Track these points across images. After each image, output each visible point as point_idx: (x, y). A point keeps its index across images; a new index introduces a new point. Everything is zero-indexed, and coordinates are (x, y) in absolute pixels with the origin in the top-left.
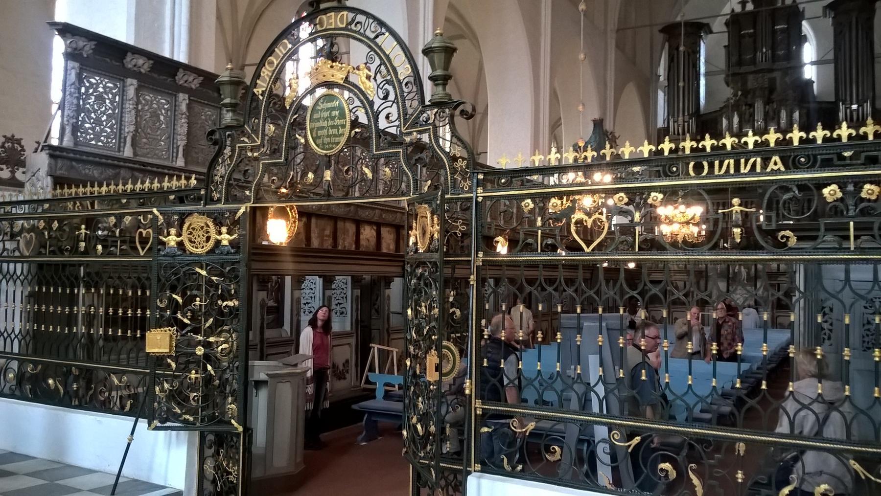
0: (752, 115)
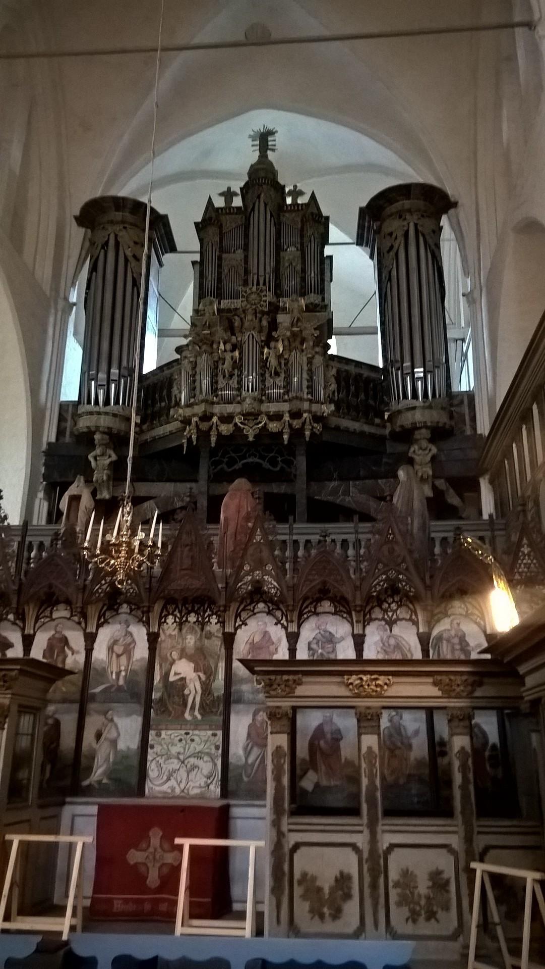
0: (238, 365)
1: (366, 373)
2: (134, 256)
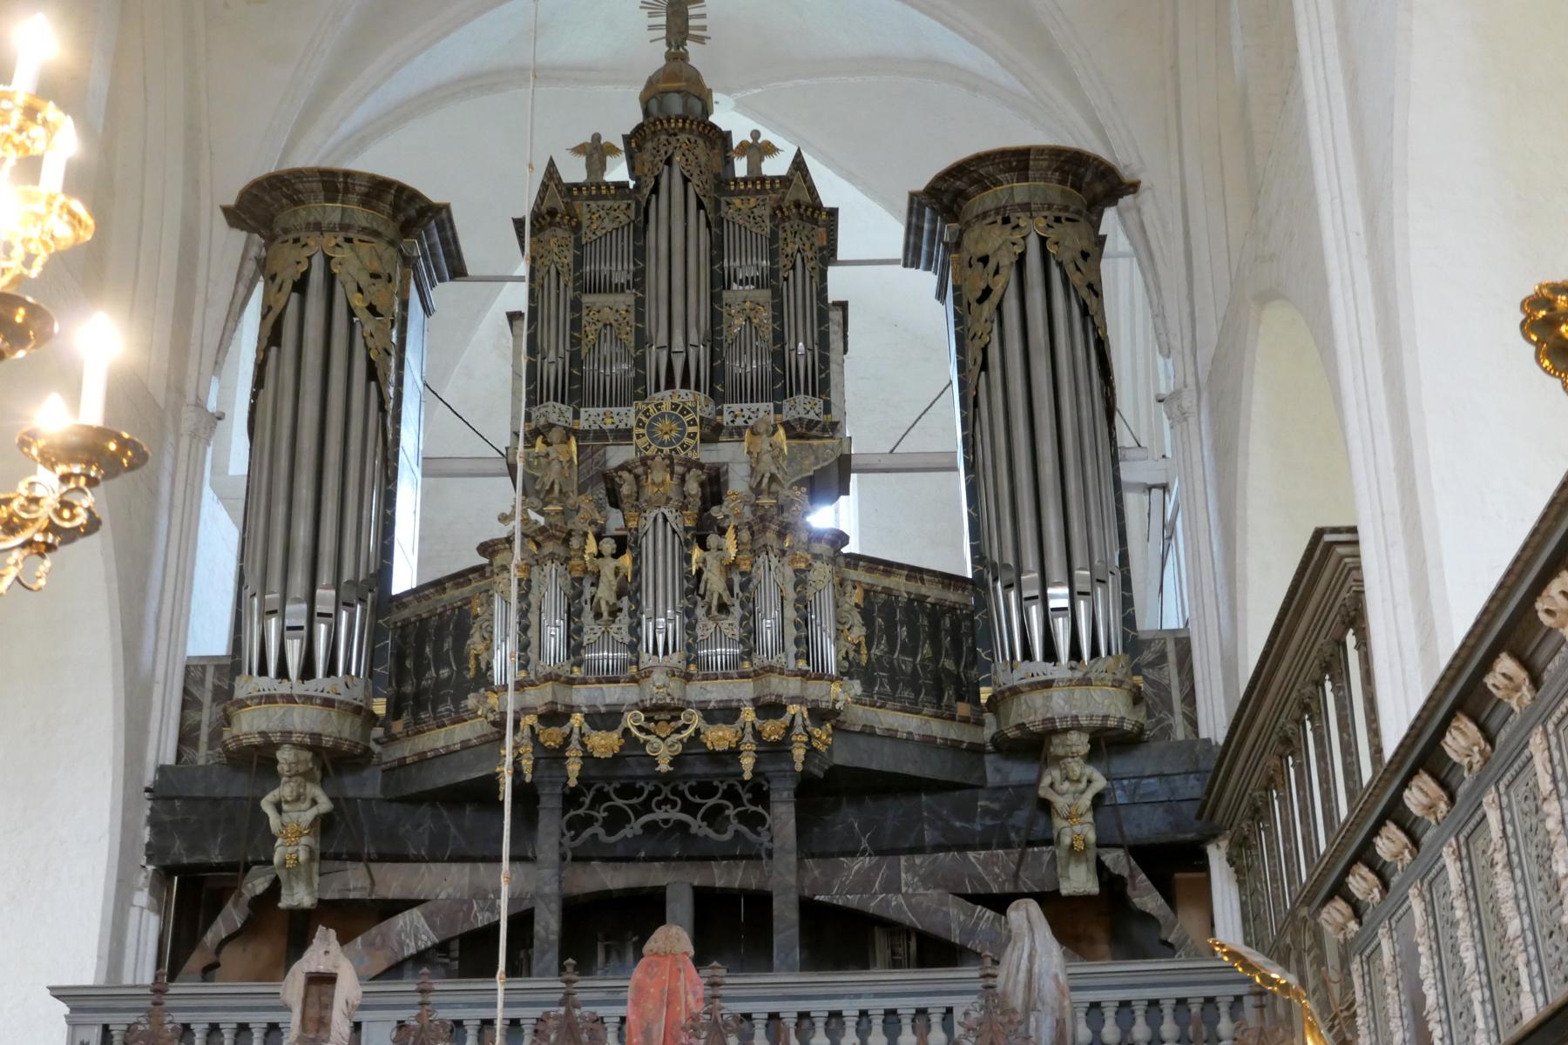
0: (629, 589)
1: (933, 592)
2: (372, 309)
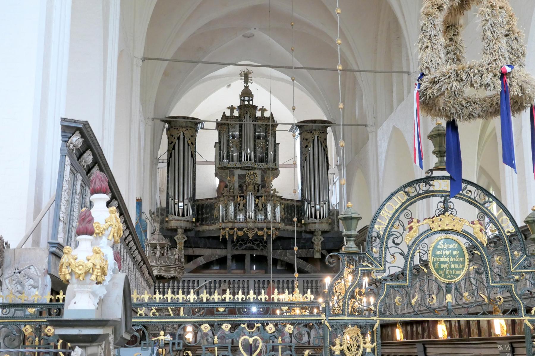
0: (245, 206)
2: (192, 143)
